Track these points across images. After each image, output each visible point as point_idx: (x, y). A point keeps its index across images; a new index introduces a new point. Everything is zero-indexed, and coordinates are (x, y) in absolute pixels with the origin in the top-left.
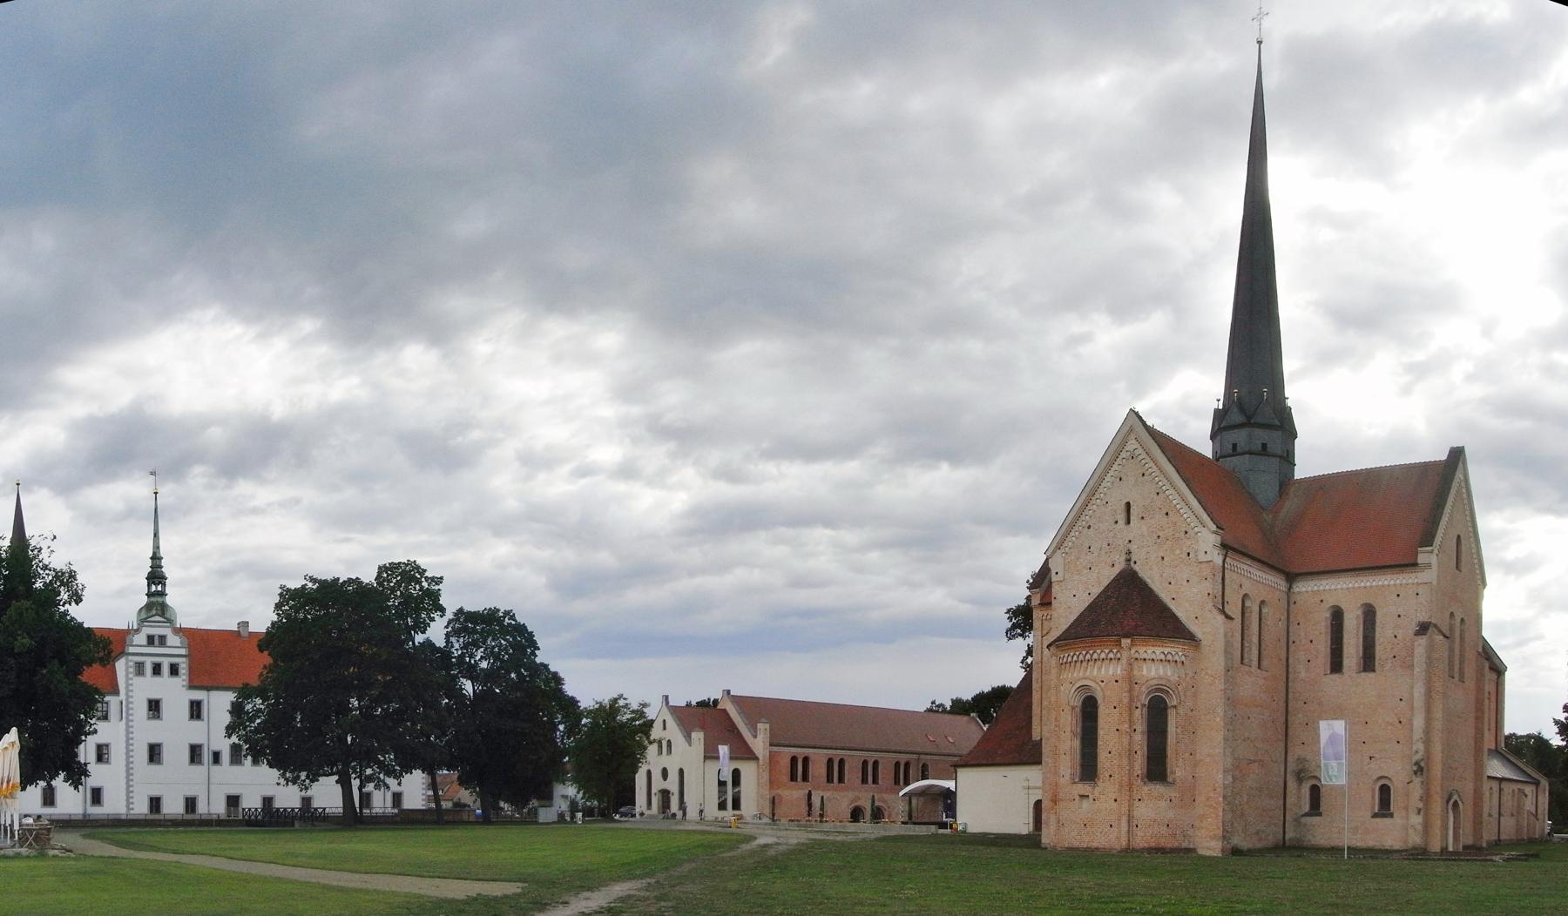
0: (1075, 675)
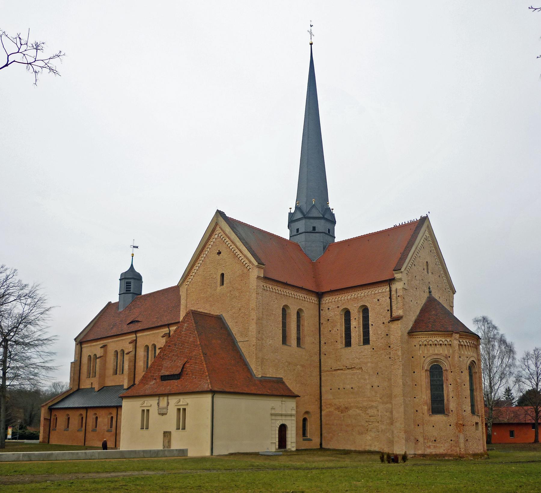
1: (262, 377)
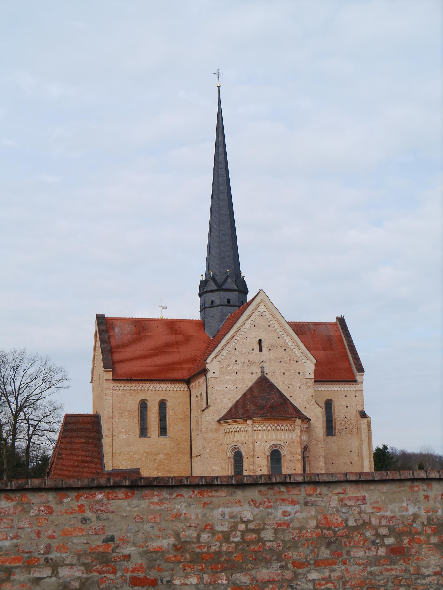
0: (269, 437)
1: (113, 470)
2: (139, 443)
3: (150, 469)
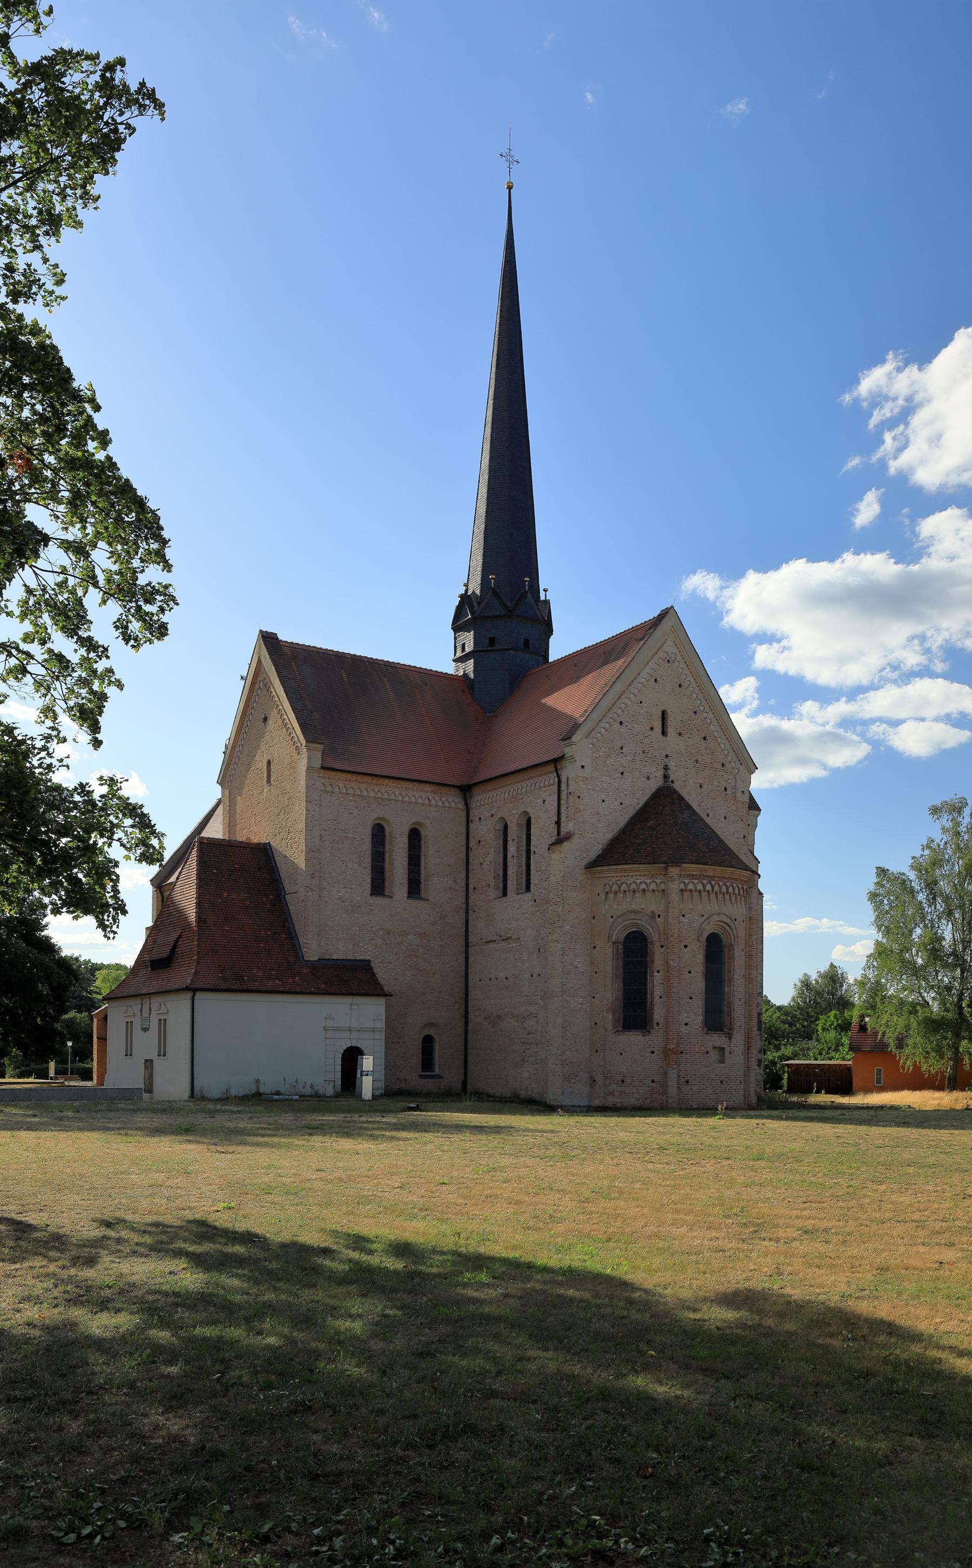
2: (371, 907)
3: (390, 963)
